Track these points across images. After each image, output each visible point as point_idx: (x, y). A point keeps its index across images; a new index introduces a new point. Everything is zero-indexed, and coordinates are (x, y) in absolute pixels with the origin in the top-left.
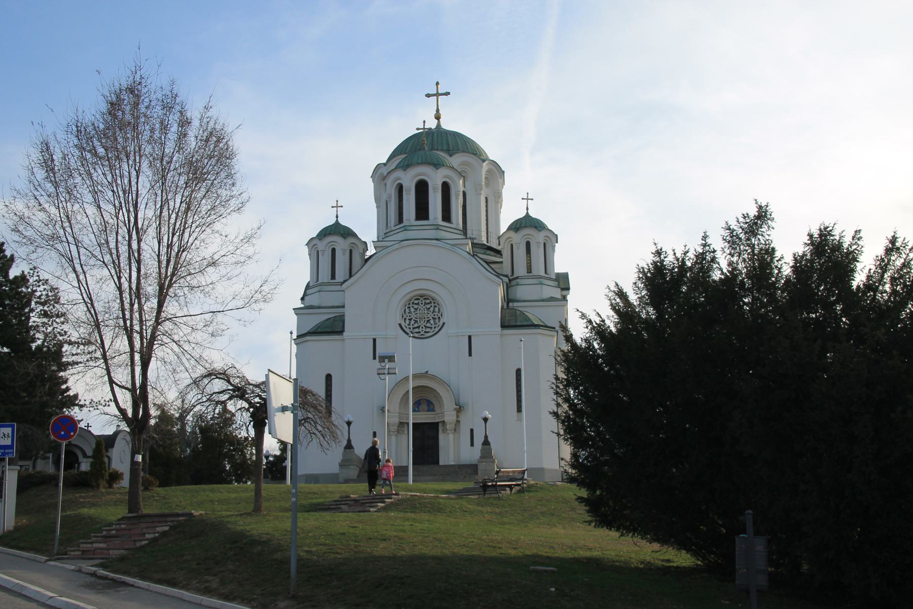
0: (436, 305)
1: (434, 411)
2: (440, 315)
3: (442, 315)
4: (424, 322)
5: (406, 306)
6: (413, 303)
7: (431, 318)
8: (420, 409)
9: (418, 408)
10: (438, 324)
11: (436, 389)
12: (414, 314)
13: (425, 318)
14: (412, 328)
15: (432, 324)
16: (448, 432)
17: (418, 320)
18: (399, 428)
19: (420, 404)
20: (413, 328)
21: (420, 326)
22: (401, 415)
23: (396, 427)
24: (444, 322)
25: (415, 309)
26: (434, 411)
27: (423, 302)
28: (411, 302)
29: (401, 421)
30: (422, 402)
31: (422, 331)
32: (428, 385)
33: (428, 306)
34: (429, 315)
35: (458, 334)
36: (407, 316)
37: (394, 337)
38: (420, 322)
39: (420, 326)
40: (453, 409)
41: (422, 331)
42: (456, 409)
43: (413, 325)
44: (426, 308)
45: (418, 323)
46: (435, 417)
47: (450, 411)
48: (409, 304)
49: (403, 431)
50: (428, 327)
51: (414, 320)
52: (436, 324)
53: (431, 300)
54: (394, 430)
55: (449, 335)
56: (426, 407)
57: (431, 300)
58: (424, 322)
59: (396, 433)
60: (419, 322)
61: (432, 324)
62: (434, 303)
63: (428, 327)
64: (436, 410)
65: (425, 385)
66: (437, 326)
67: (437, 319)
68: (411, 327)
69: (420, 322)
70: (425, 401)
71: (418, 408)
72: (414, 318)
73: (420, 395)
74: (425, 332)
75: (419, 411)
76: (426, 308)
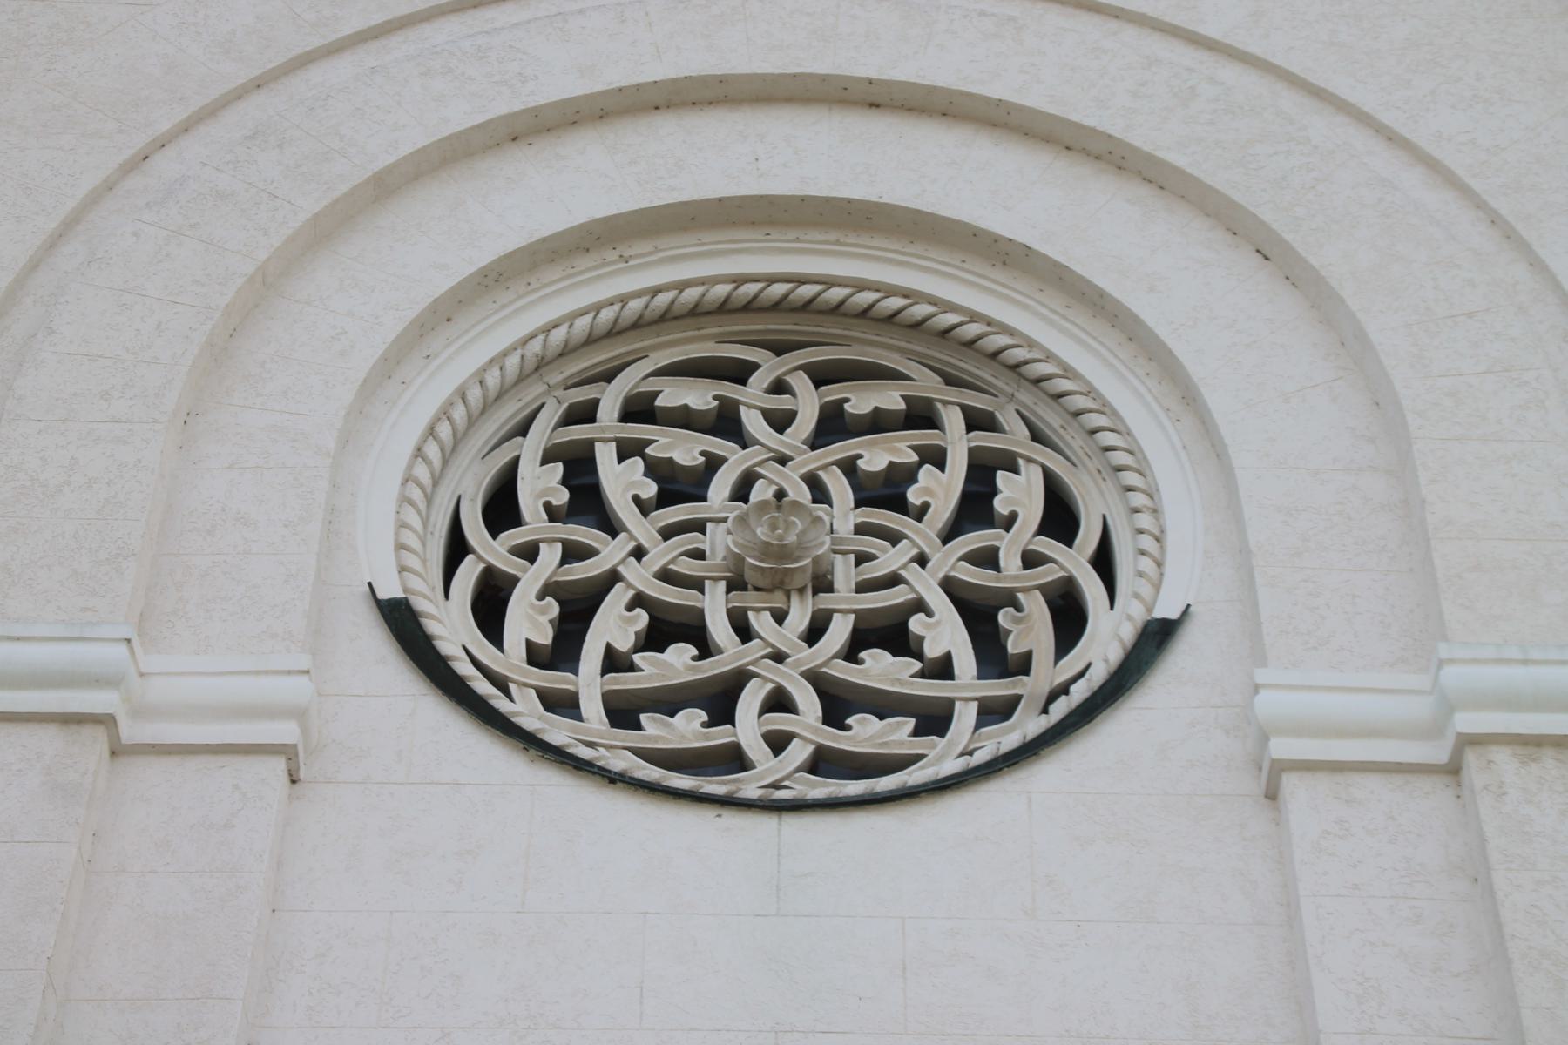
0: (1014, 437)
2: (1074, 562)
3: (1103, 562)
4: (814, 634)
5: (523, 430)
6: (639, 410)
7: (926, 586)
10: (1045, 674)
12: (640, 528)
13: (823, 584)
14: (592, 707)
15: (943, 669)
17: (715, 607)
21: (737, 681)
24: (1167, 609)
25: (658, 469)
27: (808, 404)
28: (611, 400)
31: (778, 743)
33: (876, 456)
34: (890, 559)
35: (1468, 722)
36: (529, 553)
37: (284, 732)
38: (744, 632)
39: (737, 681)
41: (778, 743)
43: (614, 662)
44: (849, 467)
45: (705, 649)
48: (585, 413)
50: (884, 705)
51: (639, 601)
52: (1024, 665)
53: (927, 385)
55: (1281, 748)
57: (927, 385)
58: (814, 634)
60: (720, 629)
62: (977, 421)
63: (884, 705)
67: (1037, 609)
68: (589, 681)
69: (744, 632)
72: (640, 577)
76: (849, 467)
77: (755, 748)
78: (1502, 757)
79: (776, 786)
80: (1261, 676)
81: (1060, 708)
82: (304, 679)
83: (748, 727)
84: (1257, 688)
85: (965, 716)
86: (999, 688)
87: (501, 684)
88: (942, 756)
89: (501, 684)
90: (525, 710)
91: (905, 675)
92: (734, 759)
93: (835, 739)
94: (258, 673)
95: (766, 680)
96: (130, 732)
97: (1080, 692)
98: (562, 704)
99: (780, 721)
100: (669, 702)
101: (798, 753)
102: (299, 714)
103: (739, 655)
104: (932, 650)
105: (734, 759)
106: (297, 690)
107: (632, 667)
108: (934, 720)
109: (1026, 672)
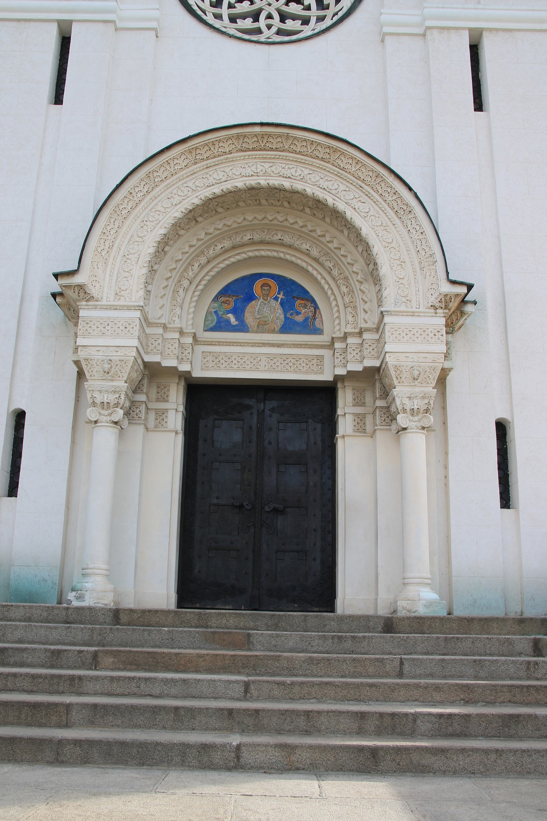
1: (318, 331)
8: (249, 318)
9: (238, 312)
10: (333, 9)
11: (341, 206)
14: (226, 18)
15: (308, 8)
16: (402, 420)
18: (142, 397)
19: (251, 298)
20: (233, 19)
21: (260, 11)
22: (148, 331)
23: (122, 385)
26: (318, 331)
29: (147, 359)
30: (257, 288)
31: (269, 27)
32: (299, 186)
35: (429, 23)
37: (154, 25)
39: (260, 11)
40: (433, 300)
41: (269, 27)
42: (446, 300)
43: (230, 6)
46: (320, 358)
47: (413, 314)
49: (161, 414)
50: (294, 18)
54: (111, 398)
55: (386, 29)
56: (280, 312)
59: (119, 414)
61: (308, 8)
63: (294, 18)
64: (327, 327)
65: (287, 184)
66: (329, 13)
70: (271, 282)
71: (238, 312)
73: (250, 252)
74: (280, 32)
75: (242, 327)
77: (264, 28)
78: (435, 32)
79: (268, 38)
80: (383, 11)
81: (336, 18)
82: (158, 11)
83: (262, 23)
84: (381, 14)
85: (313, 20)
86: (321, 13)
87: (204, 12)
88: (307, 31)
89: (204, 12)
90: (210, 19)
91: (299, 9)
92: (259, 31)
93: (283, 26)
94: (147, 9)
95: (267, 11)
96: (119, 25)
97: (340, 14)
98: (218, 17)
99: (270, 21)
100: (244, 16)
101: (274, 29)
102: (157, 20)
103: (260, 4)
104: (306, 3)
105: (259, 31)
106: (156, 13)
107: (235, 7)
108: (306, 21)
109: (328, 9)
